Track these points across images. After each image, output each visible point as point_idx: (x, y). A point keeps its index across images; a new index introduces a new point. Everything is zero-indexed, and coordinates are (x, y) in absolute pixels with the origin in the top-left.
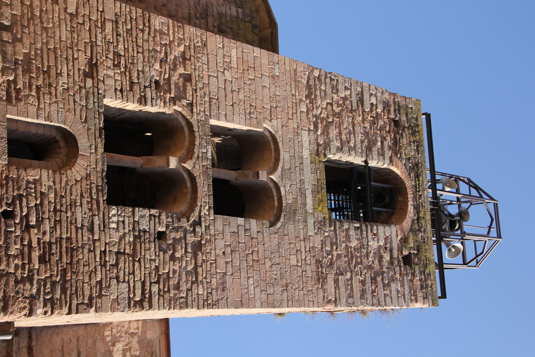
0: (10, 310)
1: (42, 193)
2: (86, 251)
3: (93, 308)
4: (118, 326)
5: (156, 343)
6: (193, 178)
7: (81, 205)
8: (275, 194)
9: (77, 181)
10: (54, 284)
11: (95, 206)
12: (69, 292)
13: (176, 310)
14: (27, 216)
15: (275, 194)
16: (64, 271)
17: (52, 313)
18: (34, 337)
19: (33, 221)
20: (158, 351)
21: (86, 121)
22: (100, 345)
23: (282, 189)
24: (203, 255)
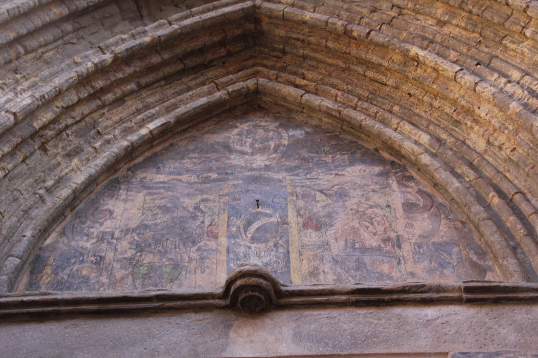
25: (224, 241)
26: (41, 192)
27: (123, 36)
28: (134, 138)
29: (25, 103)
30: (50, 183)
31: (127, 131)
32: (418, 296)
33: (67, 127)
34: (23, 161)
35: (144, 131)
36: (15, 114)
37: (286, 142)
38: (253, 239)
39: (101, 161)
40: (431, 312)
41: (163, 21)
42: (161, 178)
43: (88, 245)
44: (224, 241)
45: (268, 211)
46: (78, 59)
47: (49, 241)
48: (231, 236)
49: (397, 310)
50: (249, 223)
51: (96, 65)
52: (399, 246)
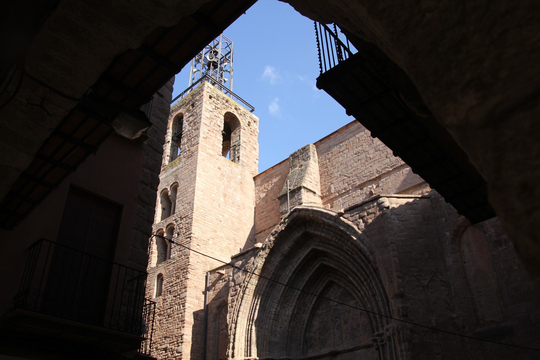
0: (186, 286)
1: (167, 283)
2: (178, 264)
3: (189, 256)
4: (256, 199)
5: (262, 178)
6: (167, 226)
7: (169, 269)
8: (173, 186)
9: (165, 272)
10: (184, 273)
11: (170, 264)
12: (185, 267)
13: (193, 223)
14: (170, 286)
15: (173, 186)
16: (181, 270)
17: (189, 271)
18: (257, 232)
19: (171, 284)
20: (264, 177)
21: (155, 272)
22: (260, 205)
23: (171, 184)
24: (182, 215)
25: (332, 330)
26: (301, 326)
27: (301, 283)
28: (313, 303)
29: (291, 313)
30: (302, 323)
31: (311, 302)
32: (358, 348)
33: (301, 307)
34: (297, 319)
35: (314, 301)
36: (290, 317)
37: (339, 294)
38: (337, 329)
39: (309, 311)
40: (359, 351)
41: (306, 274)
42: (320, 312)
43: (312, 335)
44: (332, 330)
45: (338, 320)
46: (295, 294)
47: (307, 335)
48: (333, 329)
49: (355, 352)
50: (335, 324)
51: (298, 296)
52: (359, 327)
